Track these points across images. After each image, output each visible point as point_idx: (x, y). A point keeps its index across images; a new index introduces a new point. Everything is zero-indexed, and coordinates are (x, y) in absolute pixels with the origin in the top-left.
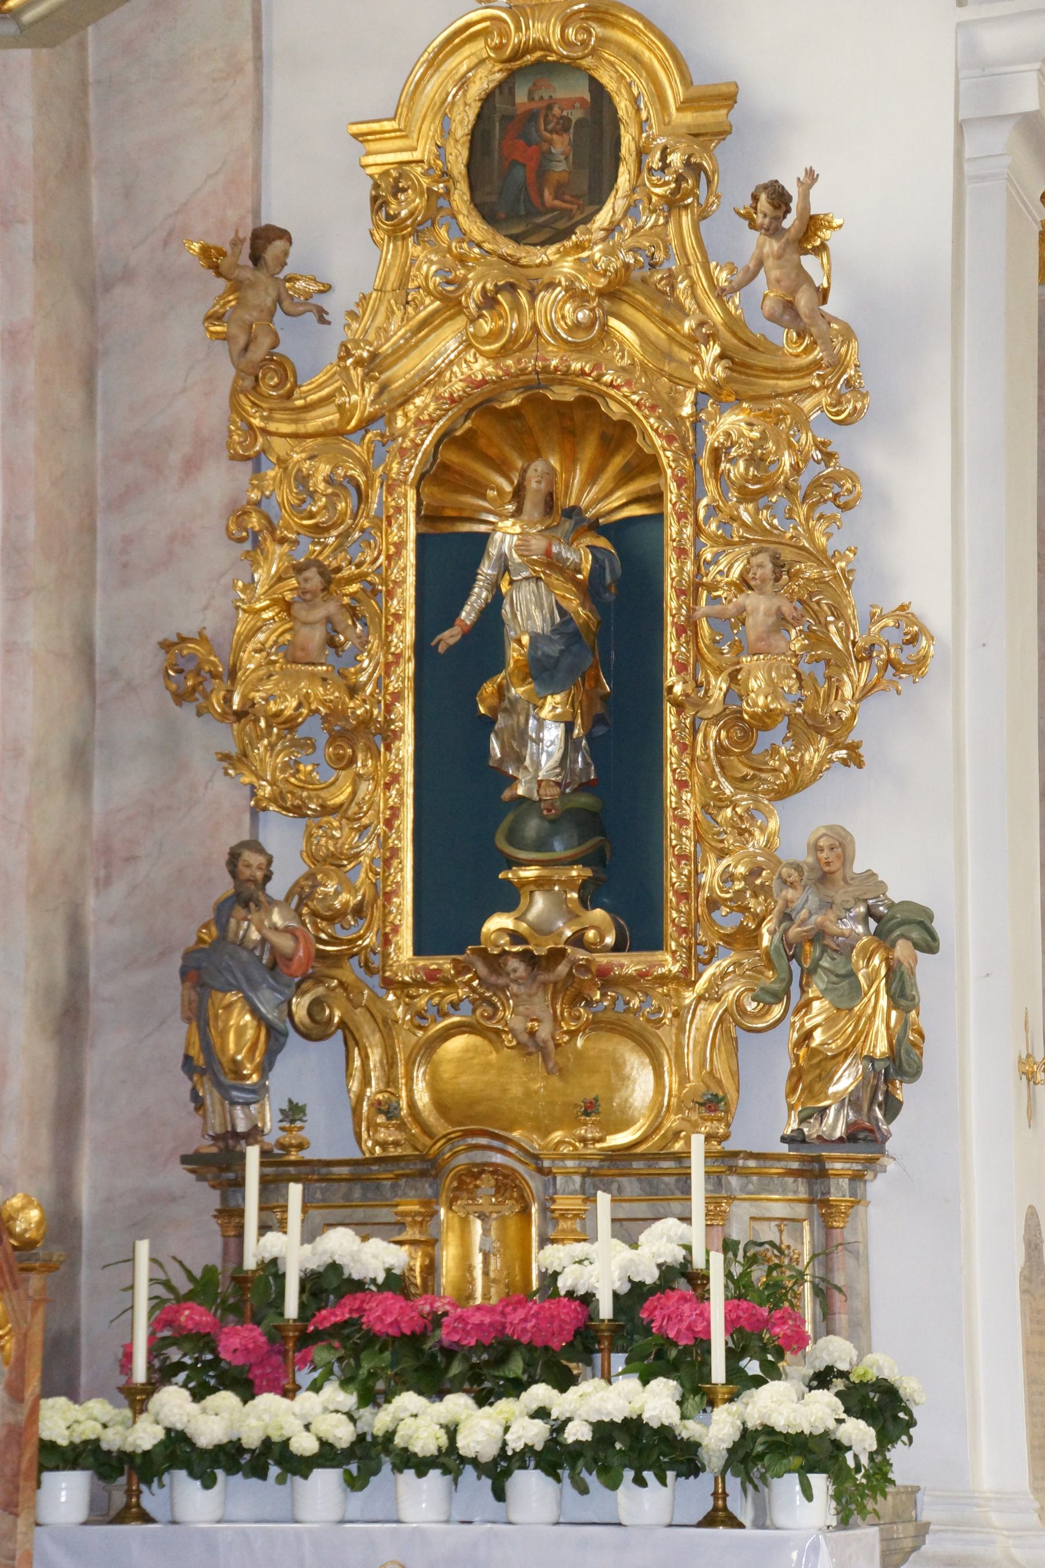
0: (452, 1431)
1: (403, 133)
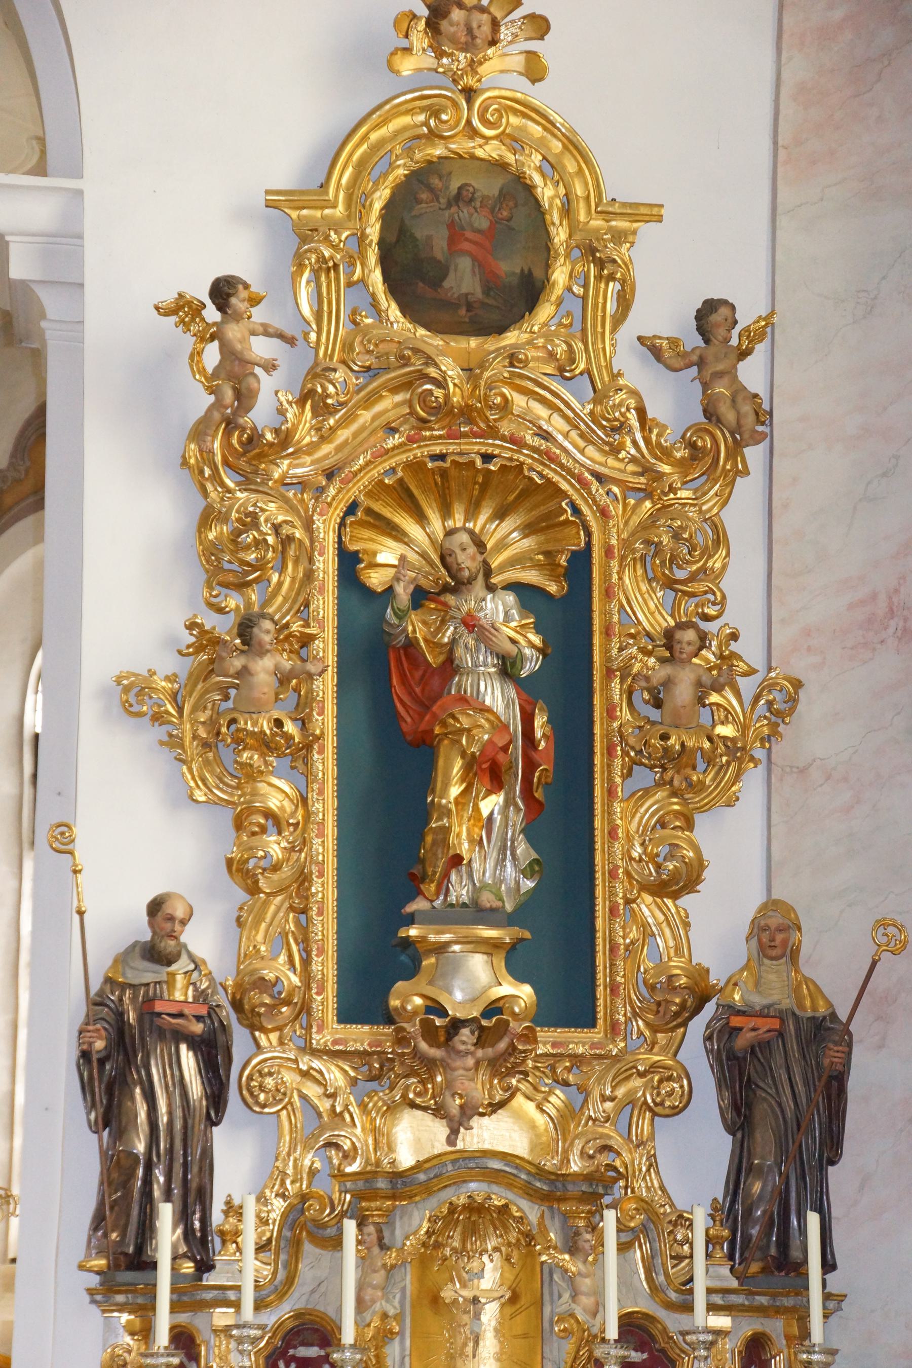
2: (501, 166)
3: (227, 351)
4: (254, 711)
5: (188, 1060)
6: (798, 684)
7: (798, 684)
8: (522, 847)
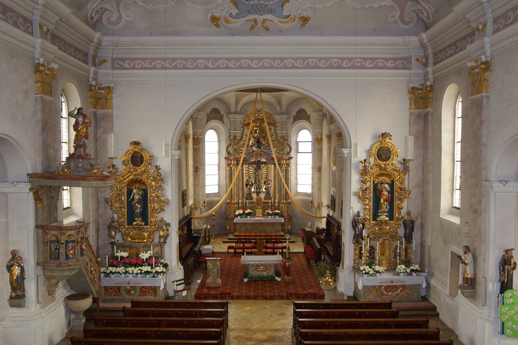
0: (133, 271)
1: (125, 157)
2: (387, 147)
3: (364, 165)
4: (366, 195)
5: (361, 225)
6: (411, 191)
7: (411, 191)
8: (388, 207)
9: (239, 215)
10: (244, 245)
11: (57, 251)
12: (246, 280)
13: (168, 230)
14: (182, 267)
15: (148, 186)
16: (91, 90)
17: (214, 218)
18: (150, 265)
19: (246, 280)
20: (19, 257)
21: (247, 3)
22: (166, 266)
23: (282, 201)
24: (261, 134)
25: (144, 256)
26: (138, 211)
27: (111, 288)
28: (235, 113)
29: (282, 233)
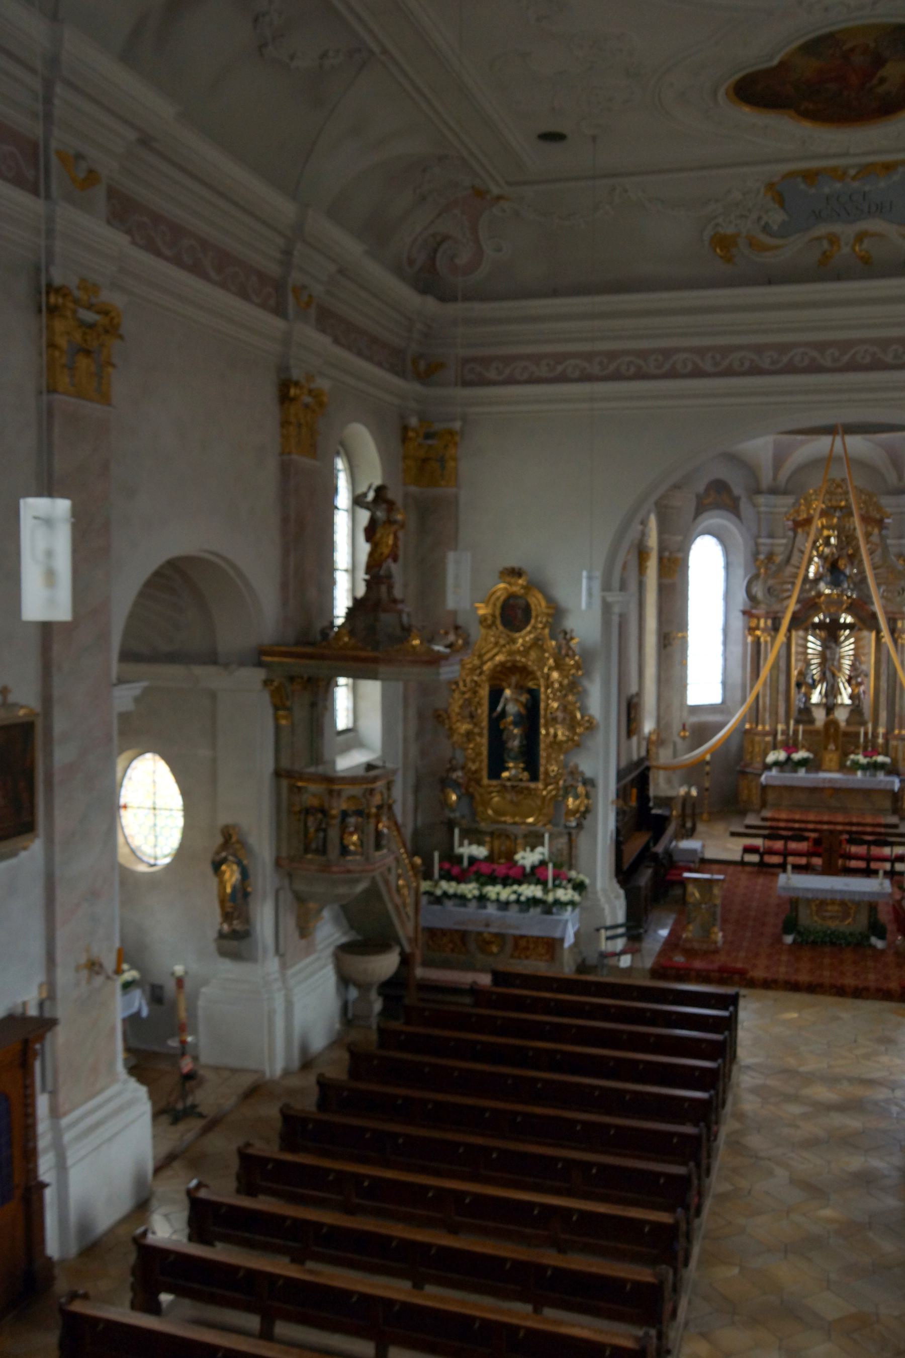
0: (498, 894)
9: (776, 764)
10: (785, 845)
11: (321, 835)
12: (789, 939)
13: (587, 796)
14: (622, 892)
15: (542, 682)
16: (404, 439)
17: (707, 768)
18: (543, 882)
19: (789, 939)
20: (238, 842)
21: (813, 191)
22: (579, 887)
23: (896, 732)
24: (842, 549)
25: (528, 858)
26: (516, 743)
27: (444, 932)
28: (774, 491)
29: (894, 820)
